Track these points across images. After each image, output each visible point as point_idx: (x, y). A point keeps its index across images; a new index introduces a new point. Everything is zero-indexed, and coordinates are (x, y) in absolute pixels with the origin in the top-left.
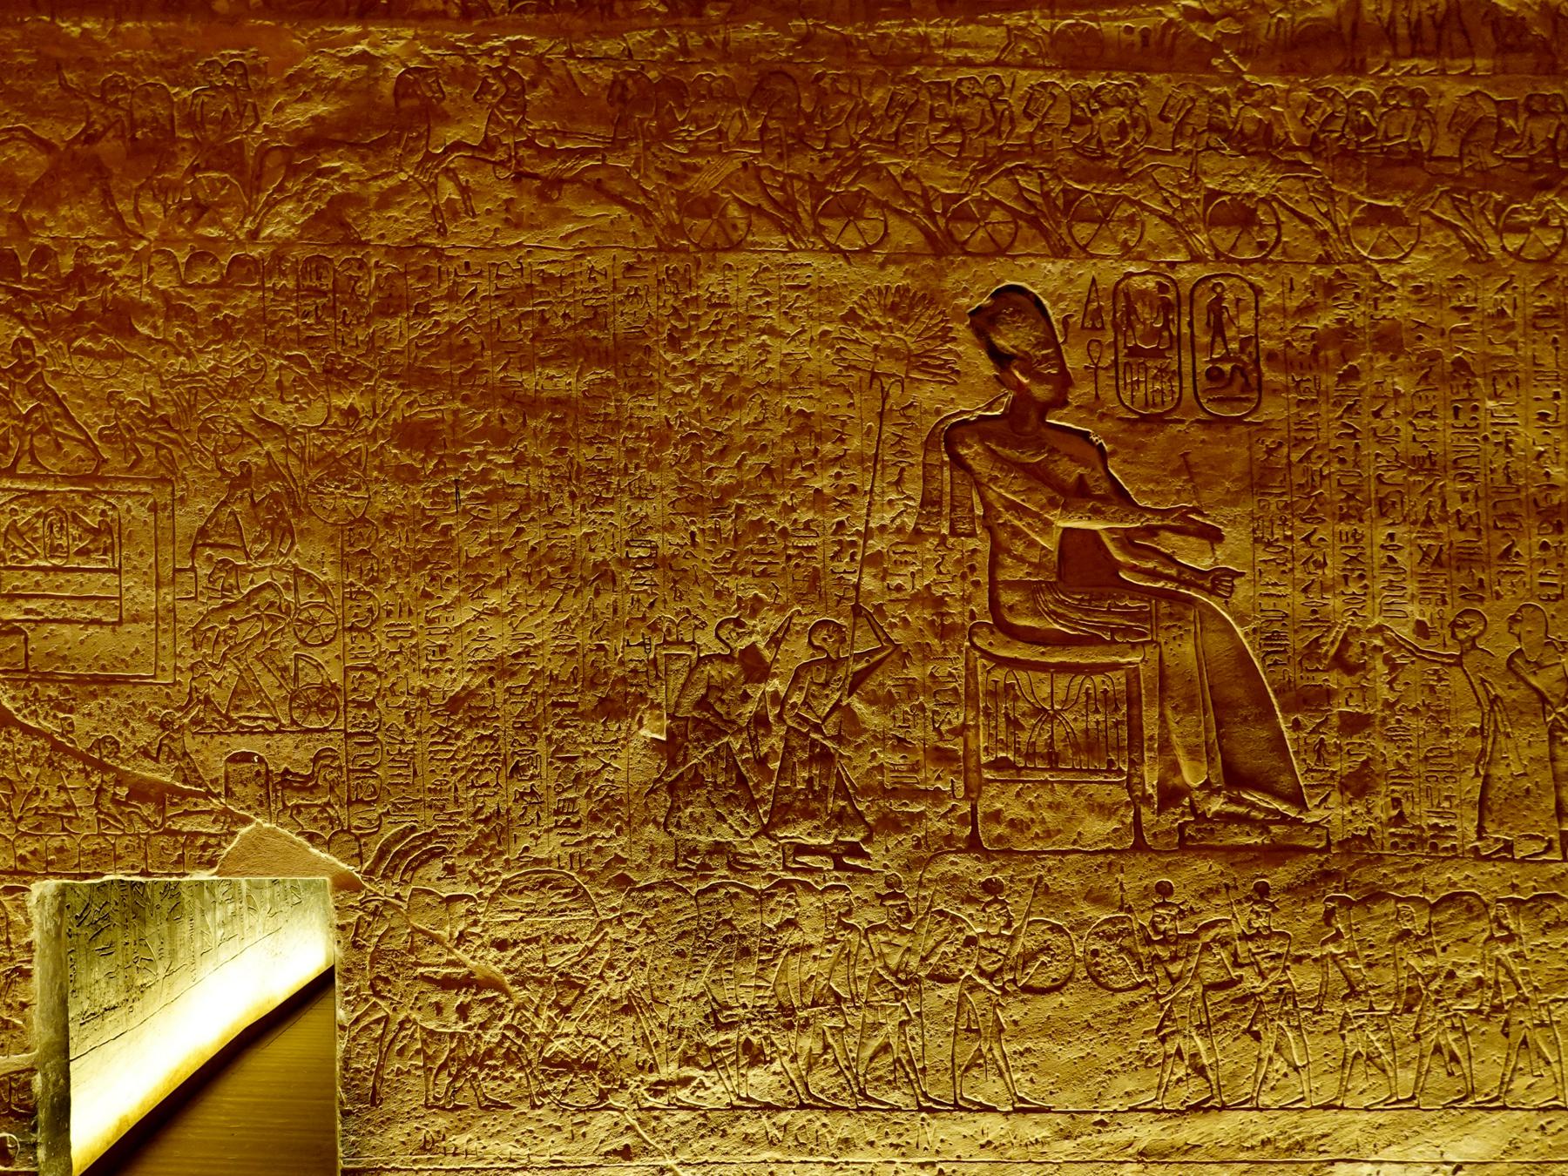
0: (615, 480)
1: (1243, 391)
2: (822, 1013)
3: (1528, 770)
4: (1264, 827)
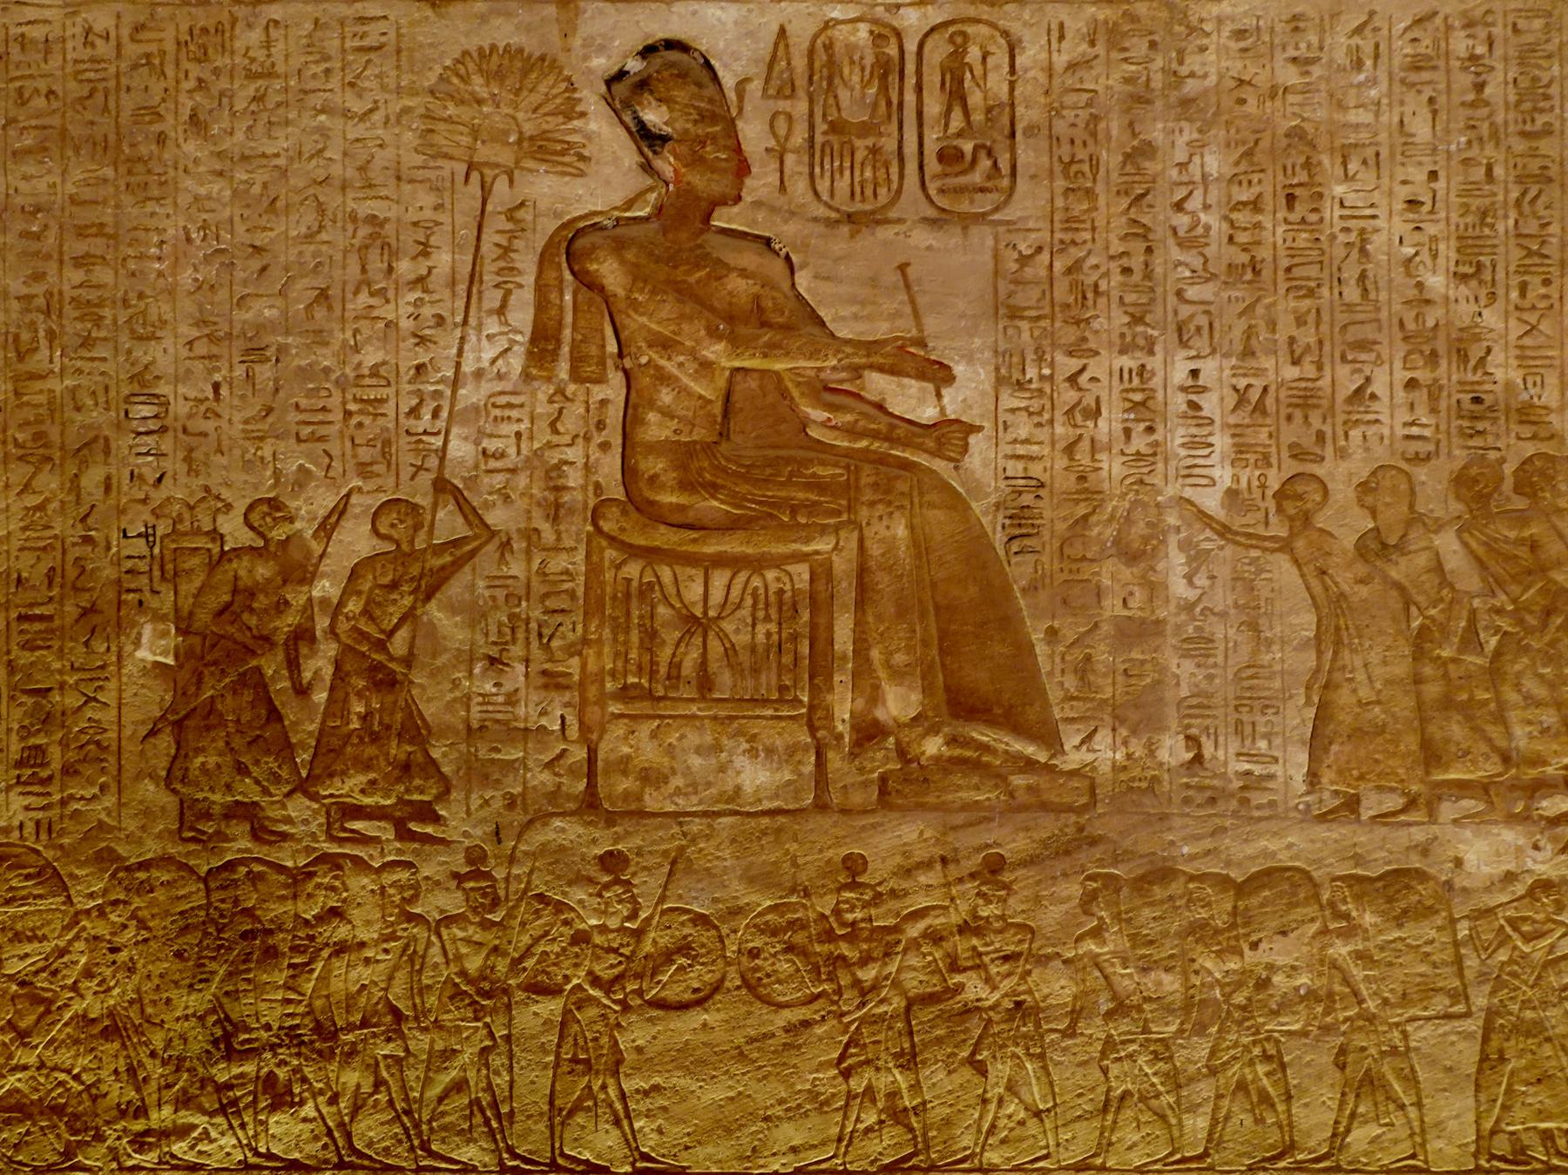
0: (107, 312)
1: (989, 178)
2: (374, 1035)
3: (1383, 697)
4: (1000, 778)
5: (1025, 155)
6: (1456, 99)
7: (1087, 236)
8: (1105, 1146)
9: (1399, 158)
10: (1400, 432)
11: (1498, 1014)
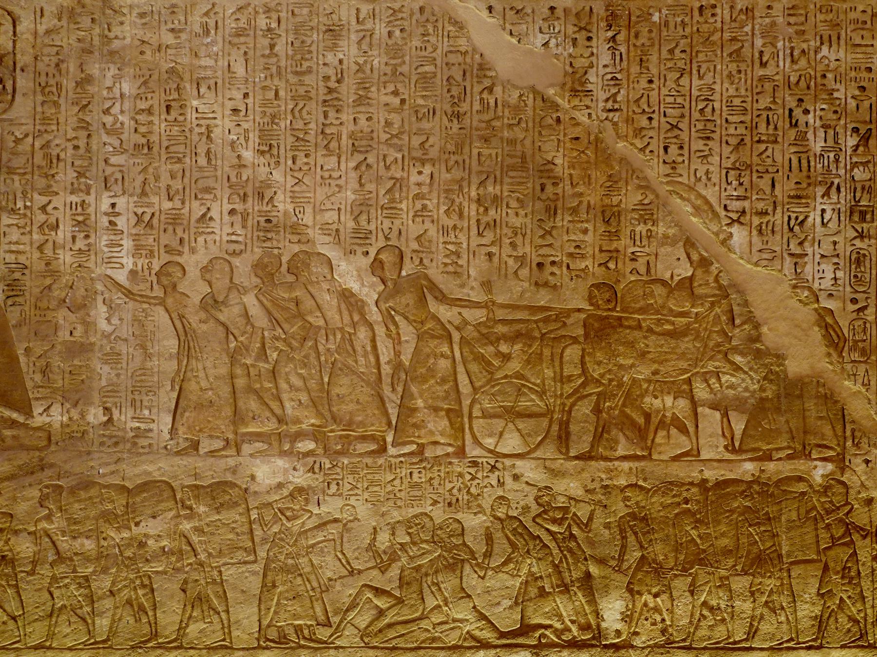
5: (21, 82)
6: (258, 54)
7: (54, 128)
8: (51, 636)
10: (225, 238)
11: (273, 561)
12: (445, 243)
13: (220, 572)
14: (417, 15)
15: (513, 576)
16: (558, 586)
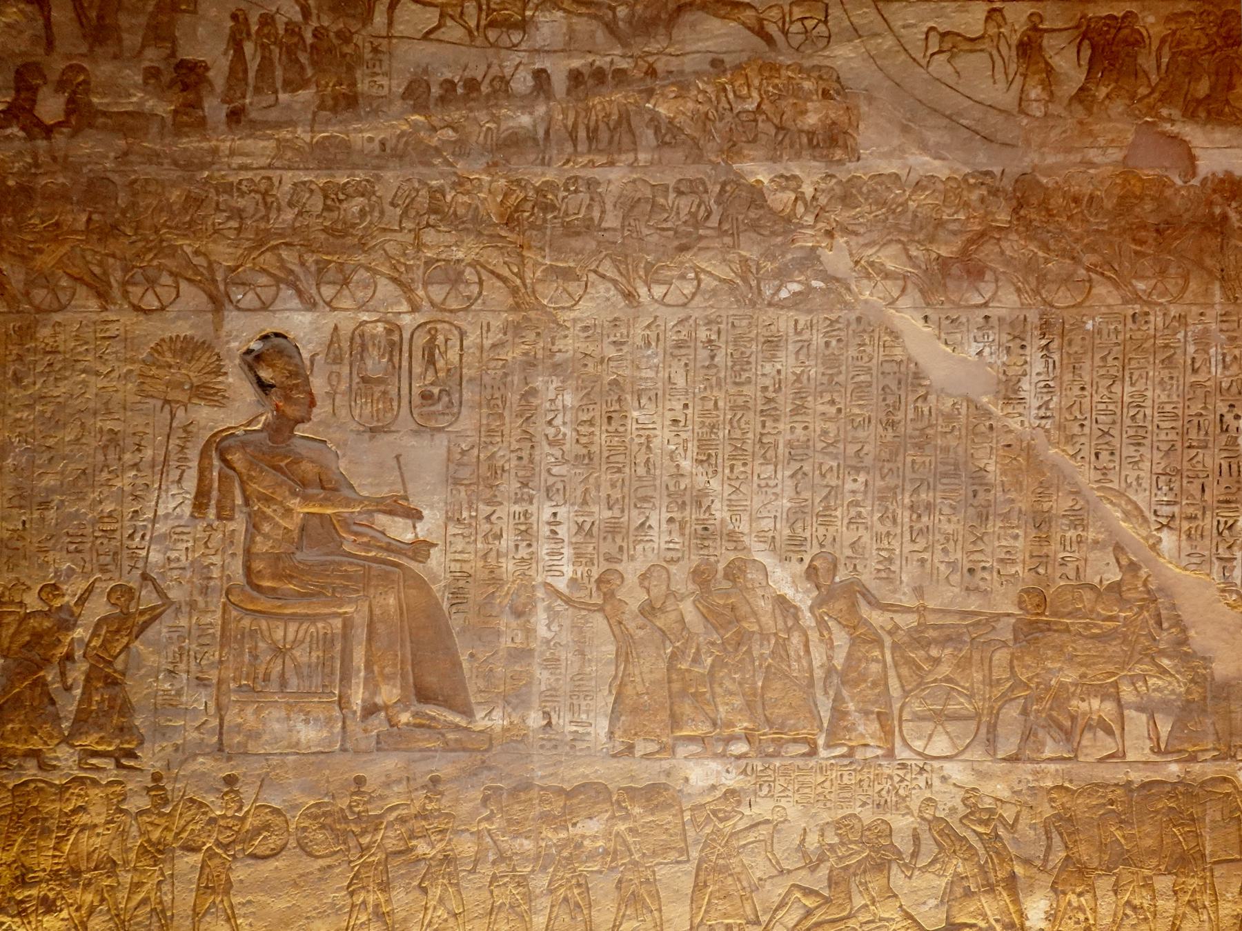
5: (467, 395)
6: (699, 365)
7: (499, 439)
9: (668, 397)
10: (664, 546)
12: (878, 549)
13: (654, 872)
14: (854, 326)
15: (939, 876)
16: (983, 886)
